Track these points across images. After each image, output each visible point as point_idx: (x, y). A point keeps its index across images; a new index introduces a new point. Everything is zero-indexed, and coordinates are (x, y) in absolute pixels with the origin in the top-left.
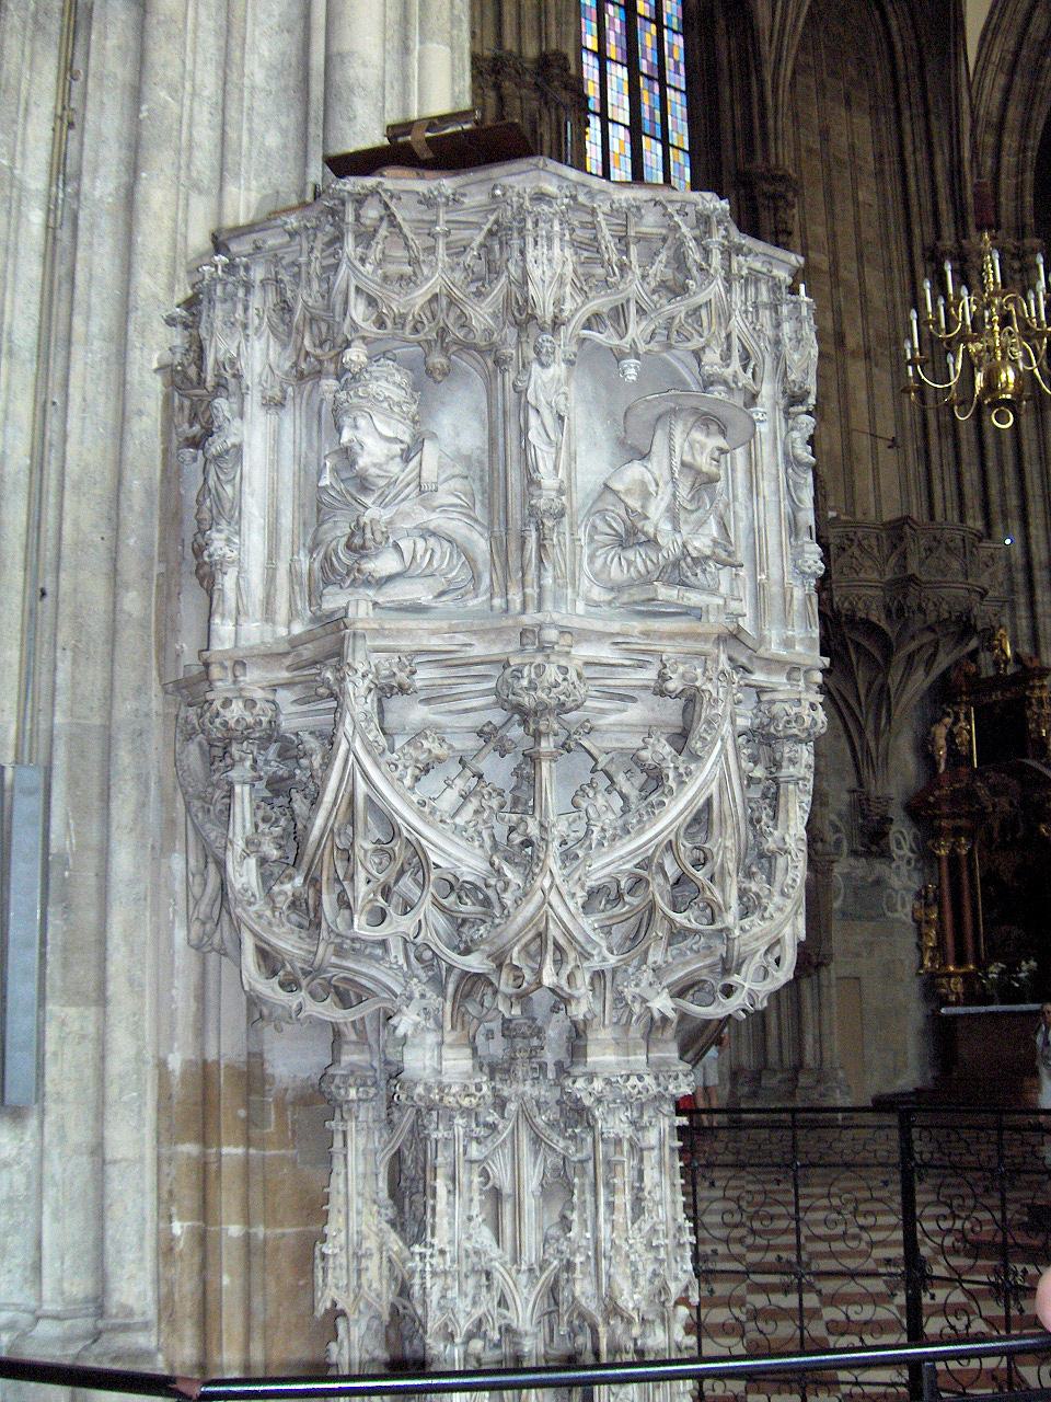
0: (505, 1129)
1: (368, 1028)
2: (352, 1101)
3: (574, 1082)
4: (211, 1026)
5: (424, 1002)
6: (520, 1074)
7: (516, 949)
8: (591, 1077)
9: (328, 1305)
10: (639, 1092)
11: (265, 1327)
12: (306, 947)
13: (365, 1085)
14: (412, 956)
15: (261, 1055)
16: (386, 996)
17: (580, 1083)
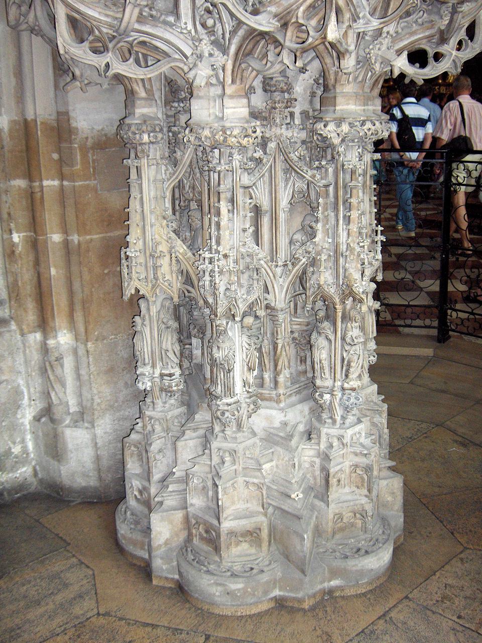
0: (268, 161)
1: (154, 88)
2: (145, 144)
3: (325, 126)
4: (28, 94)
5: (212, 59)
6: (278, 121)
7: (302, 9)
8: (339, 122)
9: (133, 292)
10: (372, 134)
11: (84, 302)
12: (111, 13)
13: (154, 131)
14: (198, 23)
15: (67, 113)
16: (177, 56)
17: (331, 127)
